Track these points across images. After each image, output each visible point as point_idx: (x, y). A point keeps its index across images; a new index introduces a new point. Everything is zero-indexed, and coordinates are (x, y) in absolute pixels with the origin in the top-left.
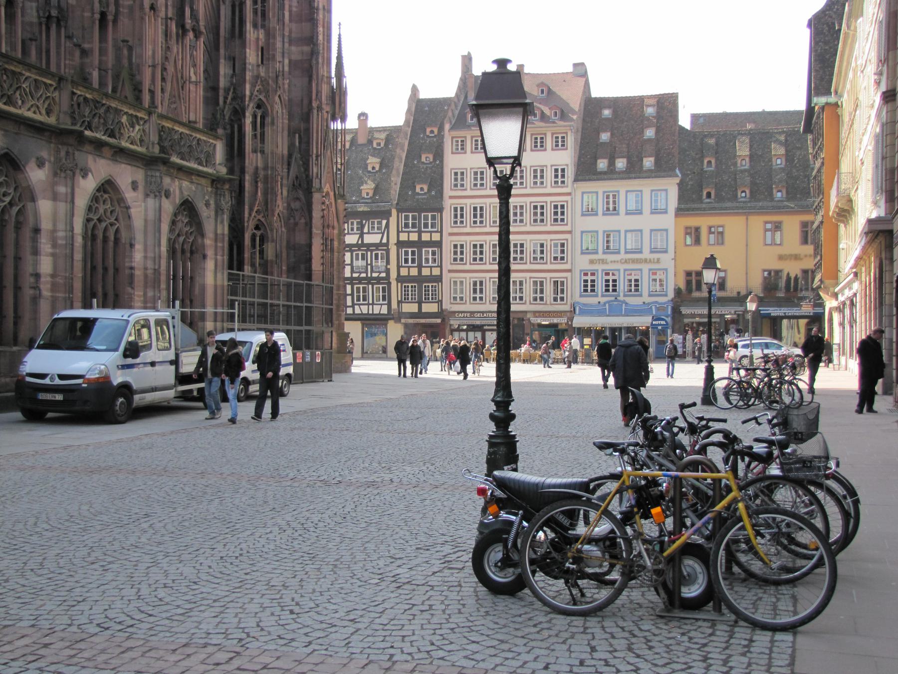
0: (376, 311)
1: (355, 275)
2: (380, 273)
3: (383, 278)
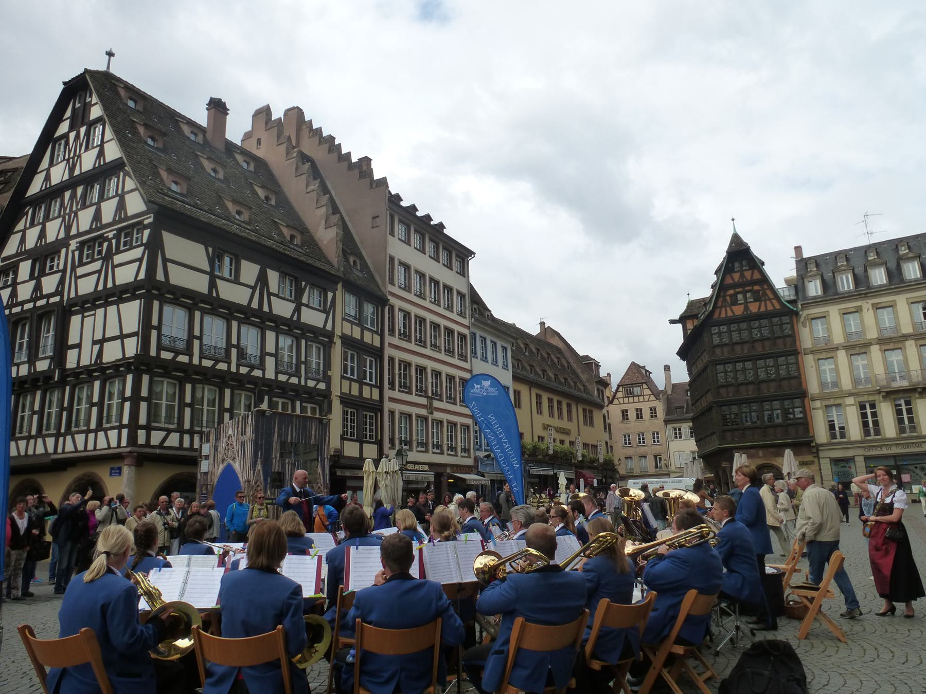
1: (282, 378)
2: (318, 381)
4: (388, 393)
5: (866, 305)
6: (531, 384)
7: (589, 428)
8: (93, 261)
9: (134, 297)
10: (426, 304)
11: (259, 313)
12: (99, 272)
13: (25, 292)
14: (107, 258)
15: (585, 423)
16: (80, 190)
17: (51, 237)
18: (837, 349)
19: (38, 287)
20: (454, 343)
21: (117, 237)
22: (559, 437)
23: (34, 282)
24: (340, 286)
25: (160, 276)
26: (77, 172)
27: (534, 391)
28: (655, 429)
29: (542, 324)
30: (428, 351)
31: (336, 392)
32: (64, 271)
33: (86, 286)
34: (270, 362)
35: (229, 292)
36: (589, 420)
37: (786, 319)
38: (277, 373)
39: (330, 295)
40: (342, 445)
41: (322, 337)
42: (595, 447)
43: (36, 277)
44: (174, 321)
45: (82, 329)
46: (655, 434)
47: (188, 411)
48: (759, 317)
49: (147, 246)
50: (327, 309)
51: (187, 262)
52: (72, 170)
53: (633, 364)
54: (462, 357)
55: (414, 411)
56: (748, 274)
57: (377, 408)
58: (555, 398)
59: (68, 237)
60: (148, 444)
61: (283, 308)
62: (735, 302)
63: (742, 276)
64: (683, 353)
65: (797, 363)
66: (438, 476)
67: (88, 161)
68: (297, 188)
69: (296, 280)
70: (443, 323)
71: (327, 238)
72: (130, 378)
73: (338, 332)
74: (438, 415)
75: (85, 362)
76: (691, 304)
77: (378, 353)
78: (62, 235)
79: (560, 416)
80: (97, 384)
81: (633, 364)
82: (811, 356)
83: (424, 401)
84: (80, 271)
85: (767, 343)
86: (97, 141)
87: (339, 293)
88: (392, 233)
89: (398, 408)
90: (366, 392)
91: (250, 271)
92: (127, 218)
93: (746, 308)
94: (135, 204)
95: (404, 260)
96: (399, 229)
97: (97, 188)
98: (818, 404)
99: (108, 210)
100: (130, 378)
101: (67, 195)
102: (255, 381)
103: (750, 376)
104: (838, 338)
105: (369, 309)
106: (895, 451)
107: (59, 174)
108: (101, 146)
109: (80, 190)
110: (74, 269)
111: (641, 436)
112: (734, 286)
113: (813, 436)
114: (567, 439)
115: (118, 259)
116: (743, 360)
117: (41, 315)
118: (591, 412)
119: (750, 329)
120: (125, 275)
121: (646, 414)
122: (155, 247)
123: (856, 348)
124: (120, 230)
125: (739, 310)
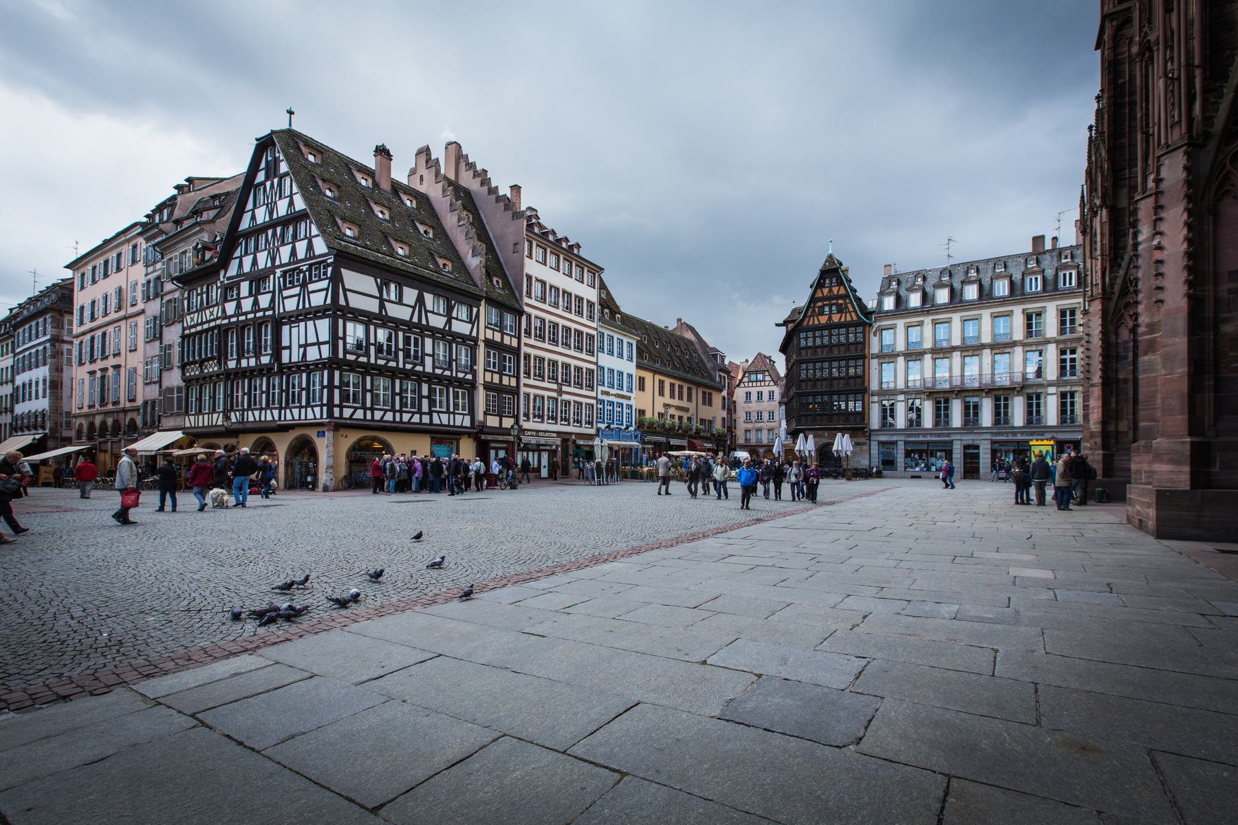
0: (458, 423)
1: (438, 371)
3: (467, 381)
4: (523, 380)
5: (927, 320)
6: (655, 372)
7: (707, 407)
8: (294, 286)
10: (559, 312)
11: (419, 325)
12: (299, 295)
13: (247, 305)
14: (304, 285)
15: (704, 403)
16: (279, 230)
17: (261, 265)
18: (898, 355)
19: (256, 303)
20: (583, 342)
21: (310, 270)
22: (677, 413)
23: (252, 299)
24: (483, 303)
25: (342, 302)
26: (275, 216)
27: (658, 377)
28: (771, 409)
29: (679, 320)
30: (559, 349)
31: (480, 380)
32: (274, 292)
33: (291, 305)
34: (428, 360)
35: (394, 311)
36: (708, 401)
37: (860, 329)
38: (434, 368)
39: (475, 310)
40: (485, 419)
41: (470, 342)
42: (710, 422)
43: (255, 293)
44: (354, 332)
45: (293, 336)
46: (771, 414)
47: (369, 395)
48: (839, 326)
49: (331, 279)
50: (473, 320)
51: (361, 288)
52: (271, 214)
53: (759, 354)
54: (591, 352)
55: (546, 394)
56: (835, 290)
57: (515, 391)
58: (677, 383)
59: (274, 267)
60: (341, 416)
61: (438, 322)
62: (822, 313)
63: (831, 291)
64: (783, 349)
65: (864, 365)
66: (565, 441)
67: (282, 208)
68: (452, 221)
69: (448, 300)
70: (573, 326)
71: (474, 263)
73: (482, 337)
74: (565, 397)
75: (295, 359)
76: (794, 311)
77: (516, 352)
78: (269, 264)
79: (681, 398)
81: (759, 354)
82: (876, 361)
83: (555, 386)
84: (286, 293)
85: (842, 348)
86: (288, 193)
87: (482, 309)
88: (530, 257)
89: (532, 391)
90: (505, 381)
91: (410, 295)
92: (315, 257)
93: (830, 318)
94: (320, 247)
95: (540, 277)
96: (537, 252)
97: (291, 228)
98: (876, 399)
99: (301, 247)
100: (326, 372)
101: (270, 232)
102: (418, 374)
103: (826, 374)
104: (901, 347)
105: (509, 319)
106: (929, 438)
107: (261, 215)
108: (291, 196)
109: (279, 230)
110: (280, 291)
111: (760, 414)
112: (823, 299)
113: (868, 424)
114: (685, 416)
115: (311, 287)
116: (822, 361)
117: (259, 324)
118: (710, 394)
119: (830, 335)
120: (317, 300)
121: (766, 396)
122: (336, 280)
123: (913, 355)
124: (311, 265)
125: (823, 320)
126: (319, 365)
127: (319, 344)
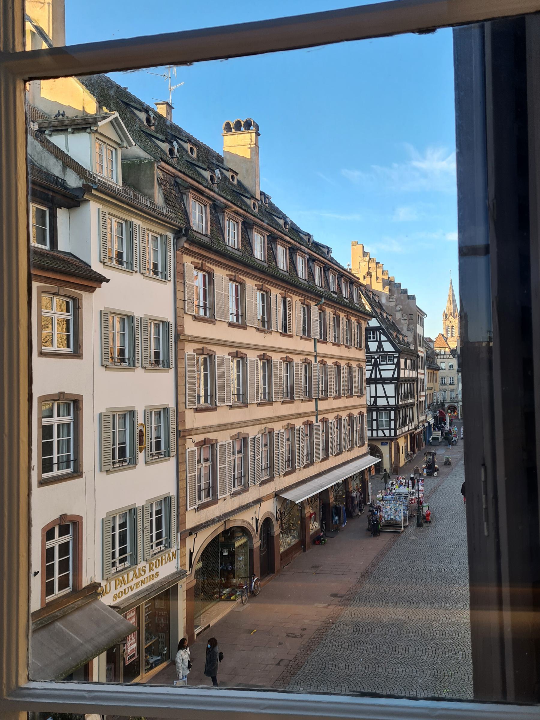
9: (391, 383)
12: (372, 371)
14: (376, 365)
72: (392, 413)
80: (375, 413)
100: (392, 413)
115: (381, 367)
126: (387, 408)
127: (386, 397)
